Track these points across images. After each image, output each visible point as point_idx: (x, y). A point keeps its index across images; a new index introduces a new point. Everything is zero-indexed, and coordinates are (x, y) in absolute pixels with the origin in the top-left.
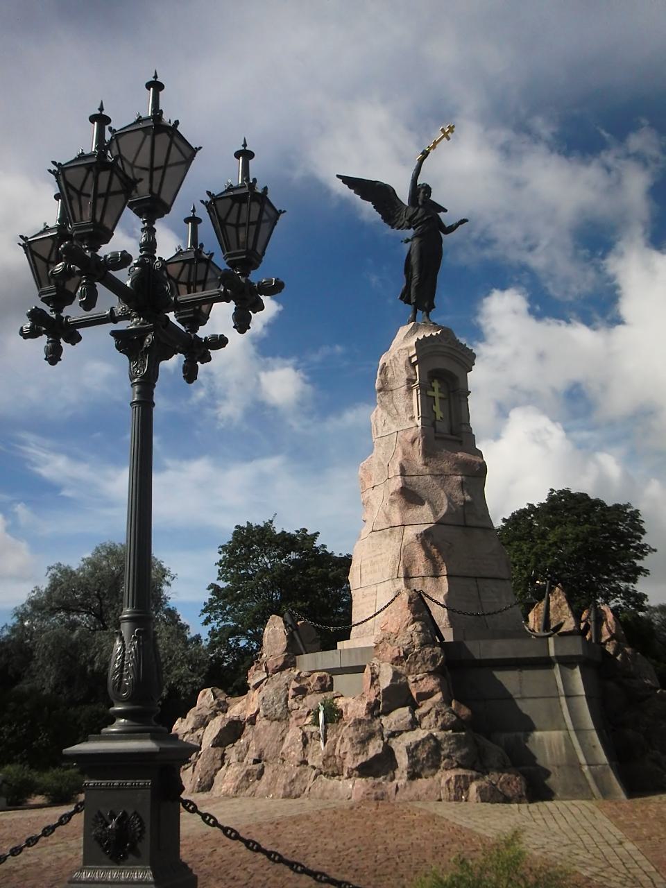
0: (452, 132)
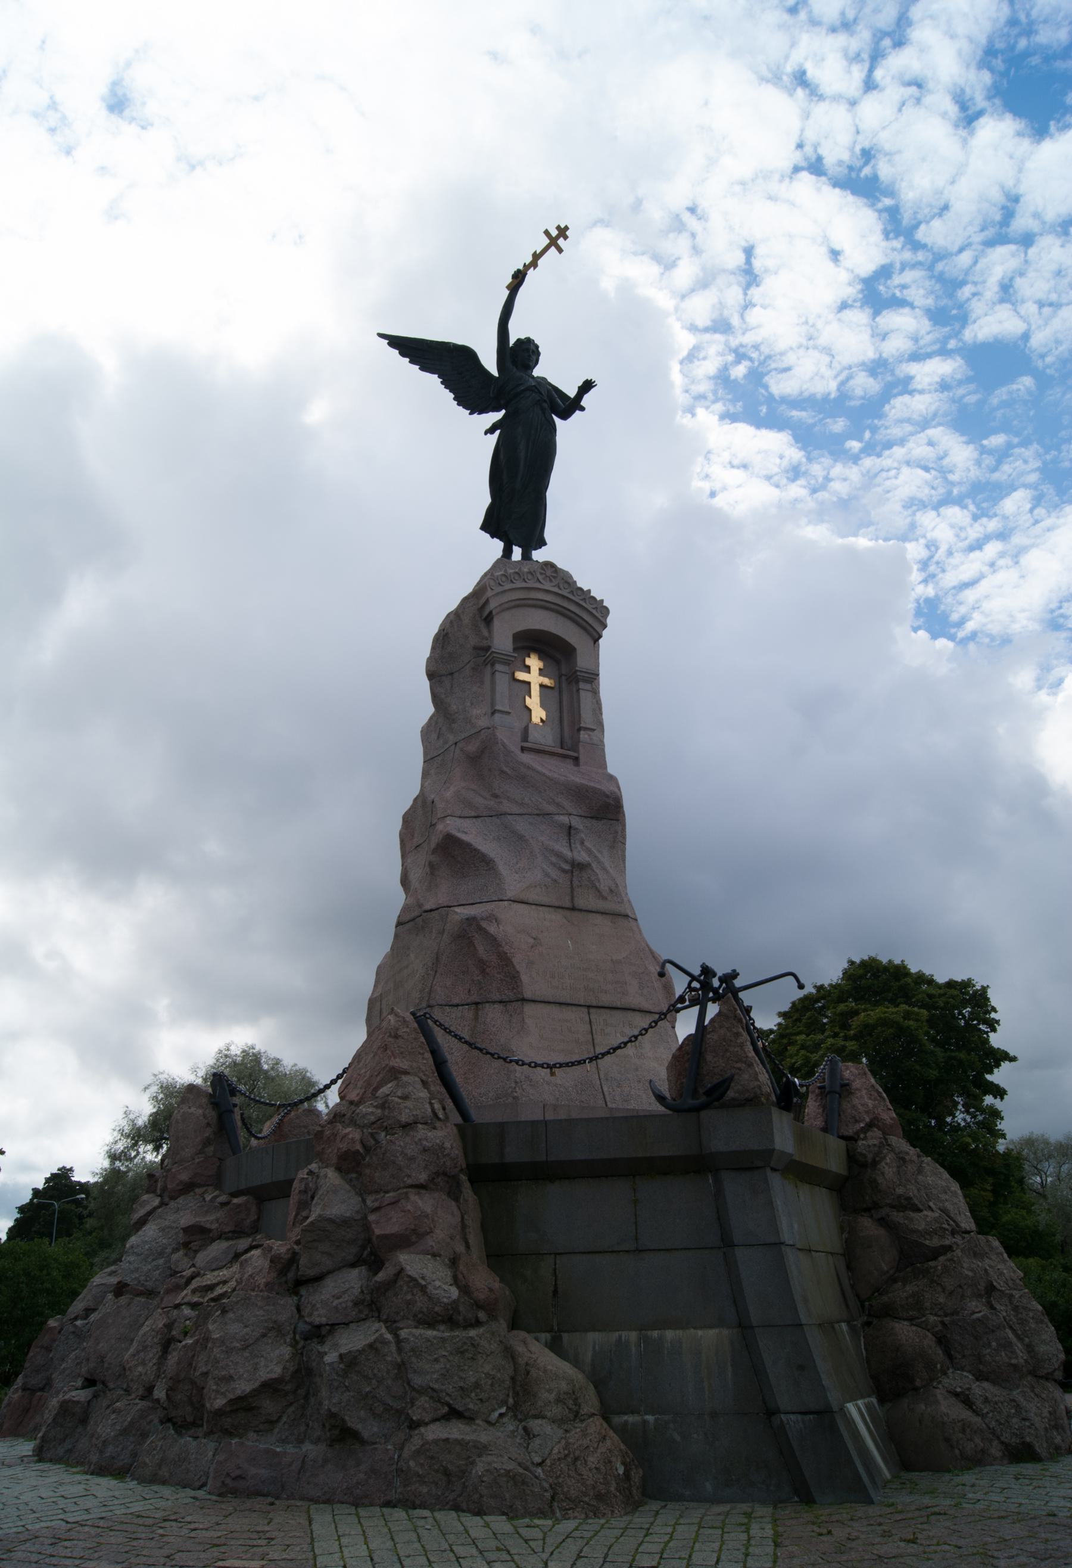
0: (566, 238)
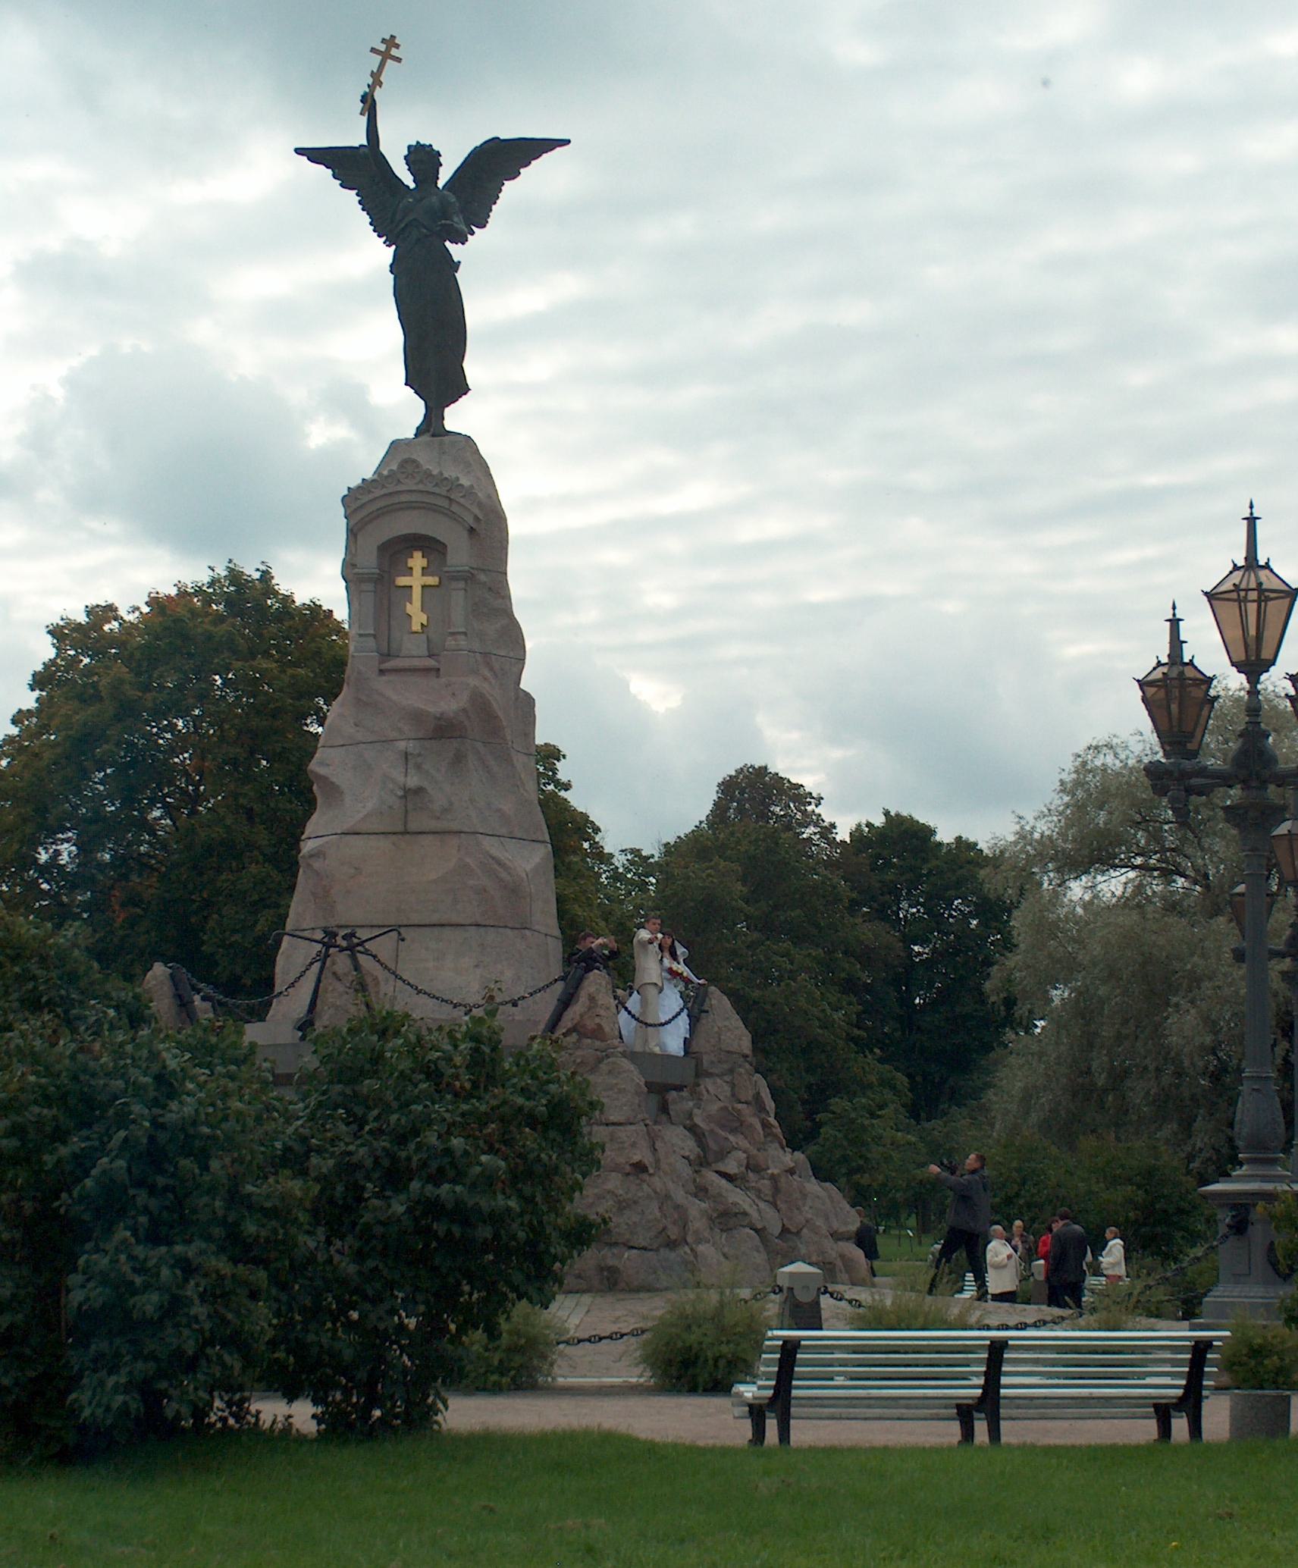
0: (397, 46)
